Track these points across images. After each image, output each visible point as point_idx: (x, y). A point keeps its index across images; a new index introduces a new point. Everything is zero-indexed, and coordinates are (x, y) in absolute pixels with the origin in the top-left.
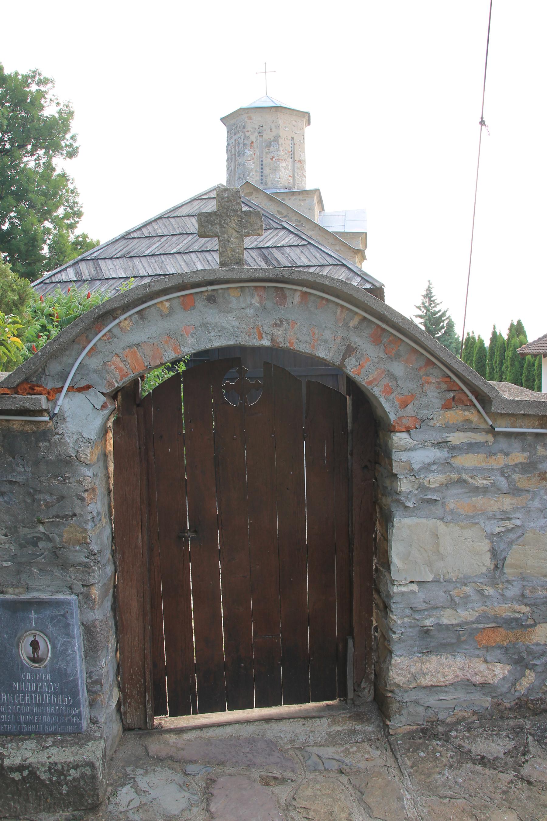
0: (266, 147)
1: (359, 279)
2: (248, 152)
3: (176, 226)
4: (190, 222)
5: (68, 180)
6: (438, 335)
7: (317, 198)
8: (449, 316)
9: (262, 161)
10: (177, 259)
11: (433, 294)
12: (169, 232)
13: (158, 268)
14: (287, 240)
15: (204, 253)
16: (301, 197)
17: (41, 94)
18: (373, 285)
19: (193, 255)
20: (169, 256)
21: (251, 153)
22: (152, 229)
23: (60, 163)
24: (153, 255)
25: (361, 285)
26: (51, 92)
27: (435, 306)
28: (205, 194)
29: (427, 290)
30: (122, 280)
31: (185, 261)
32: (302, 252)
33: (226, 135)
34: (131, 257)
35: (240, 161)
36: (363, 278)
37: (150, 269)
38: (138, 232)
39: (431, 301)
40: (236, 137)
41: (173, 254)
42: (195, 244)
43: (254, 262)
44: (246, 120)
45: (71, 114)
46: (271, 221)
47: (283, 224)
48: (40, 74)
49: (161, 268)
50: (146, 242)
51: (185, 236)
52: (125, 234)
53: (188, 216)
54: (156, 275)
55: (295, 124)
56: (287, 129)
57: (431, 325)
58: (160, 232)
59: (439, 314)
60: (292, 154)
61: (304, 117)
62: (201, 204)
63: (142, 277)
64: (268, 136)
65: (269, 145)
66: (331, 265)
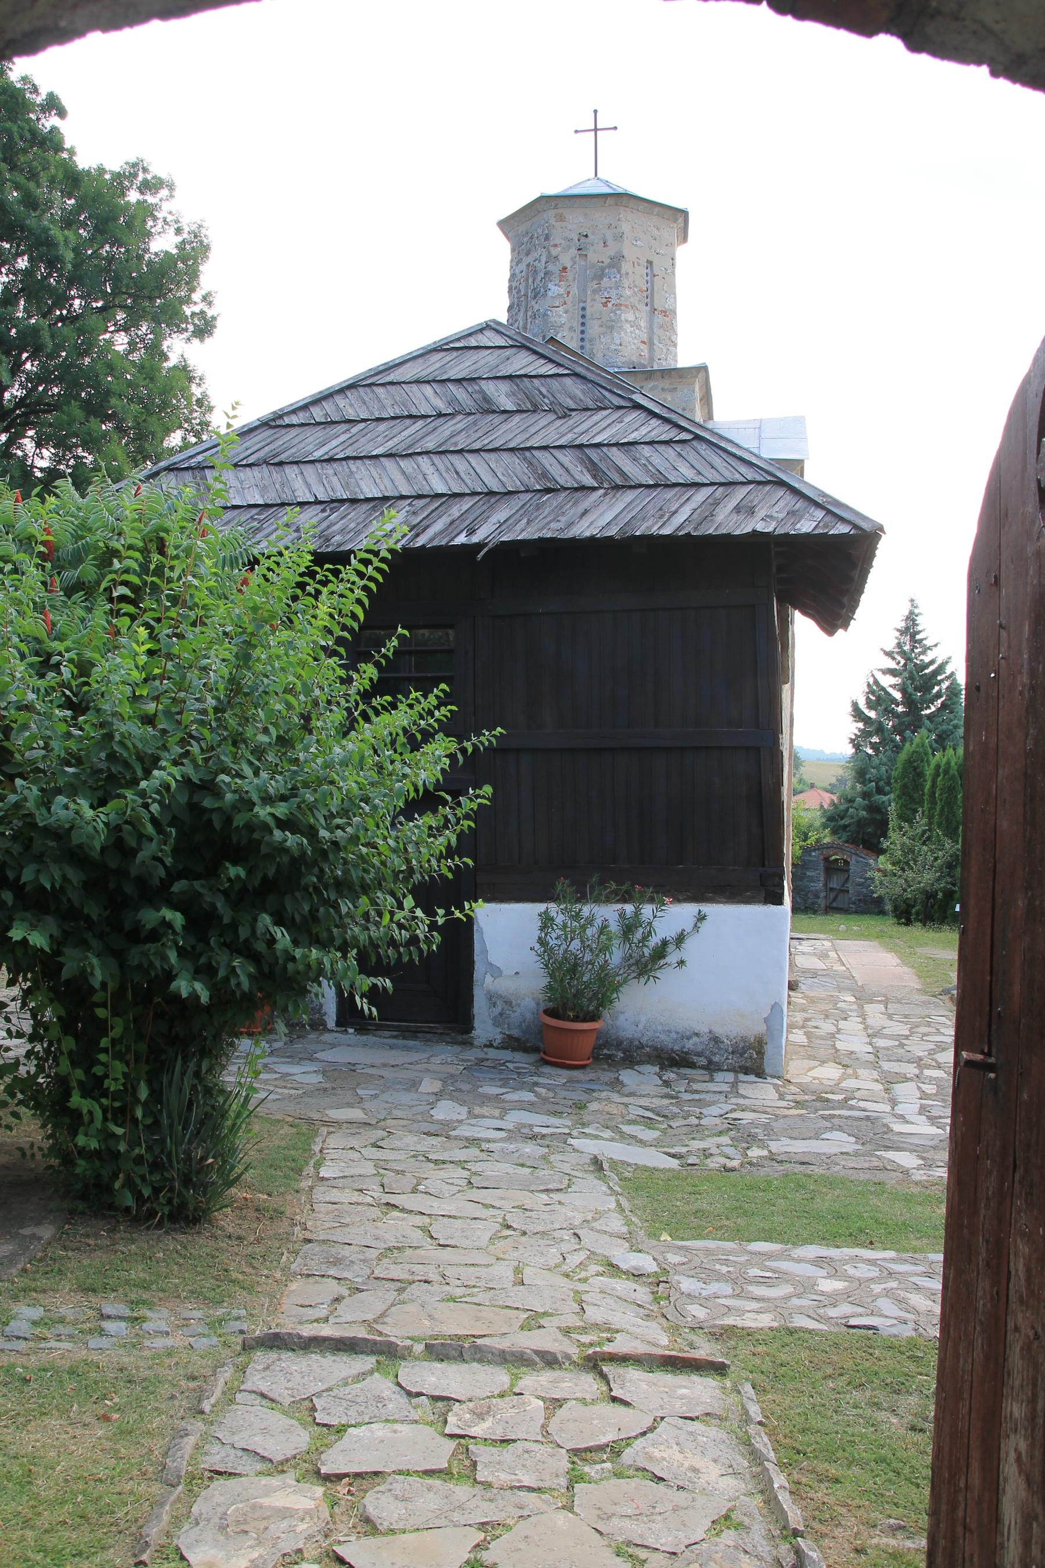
0: (593, 280)
1: (820, 514)
2: (554, 290)
3: (388, 402)
4: (419, 395)
5: (191, 379)
6: (928, 712)
7: (701, 388)
8: (952, 674)
9: (584, 309)
10: (384, 468)
11: (919, 628)
12: (372, 414)
13: (338, 487)
14: (644, 430)
15: (449, 456)
16: (665, 383)
17: (148, 211)
18: (855, 526)
19: (424, 462)
20: (367, 462)
21: (562, 291)
22: (333, 408)
23: (178, 348)
24: (331, 460)
25: (826, 526)
26: (167, 207)
27: (924, 653)
28: (458, 340)
29: (907, 618)
30: (254, 511)
31: (403, 473)
32: (680, 455)
33: (509, 257)
34: (281, 464)
35: (536, 307)
36: (829, 512)
37: (322, 489)
38: (301, 414)
39: (916, 642)
40: (529, 259)
41: (376, 457)
42: (428, 438)
43: (565, 474)
44: (552, 221)
45: (204, 249)
46: (606, 394)
47: (634, 397)
48: (145, 170)
49: (346, 486)
50: (319, 434)
51: (408, 422)
52: (272, 417)
53: (418, 382)
54: (333, 501)
55: (656, 233)
57: (916, 689)
58: (351, 414)
59: (932, 668)
60: (649, 296)
61: (675, 221)
62: (448, 358)
63: (301, 504)
64: (597, 255)
65: (599, 276)
66: (750, 482)
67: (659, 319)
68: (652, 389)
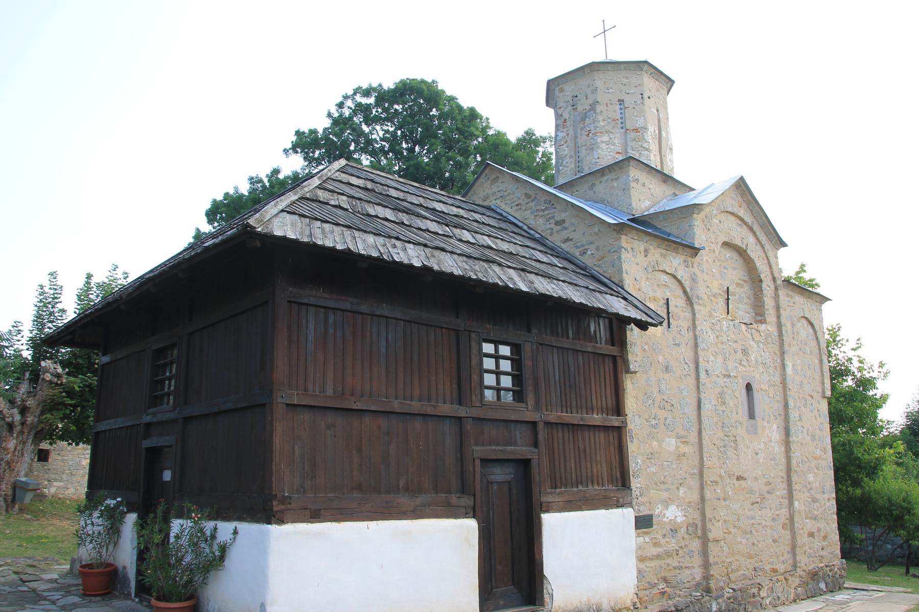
21: (564, 134)
55: (626, 81)
56: (610, 91)
64: (583, 105)
67: (633, 135)
68: (607, 181)
